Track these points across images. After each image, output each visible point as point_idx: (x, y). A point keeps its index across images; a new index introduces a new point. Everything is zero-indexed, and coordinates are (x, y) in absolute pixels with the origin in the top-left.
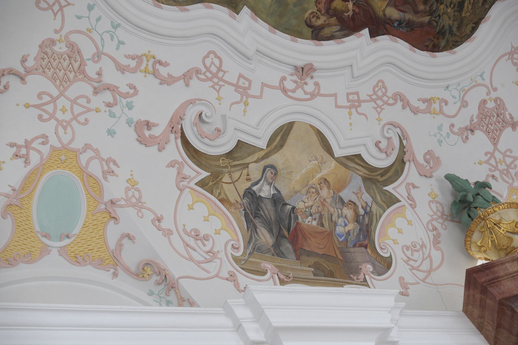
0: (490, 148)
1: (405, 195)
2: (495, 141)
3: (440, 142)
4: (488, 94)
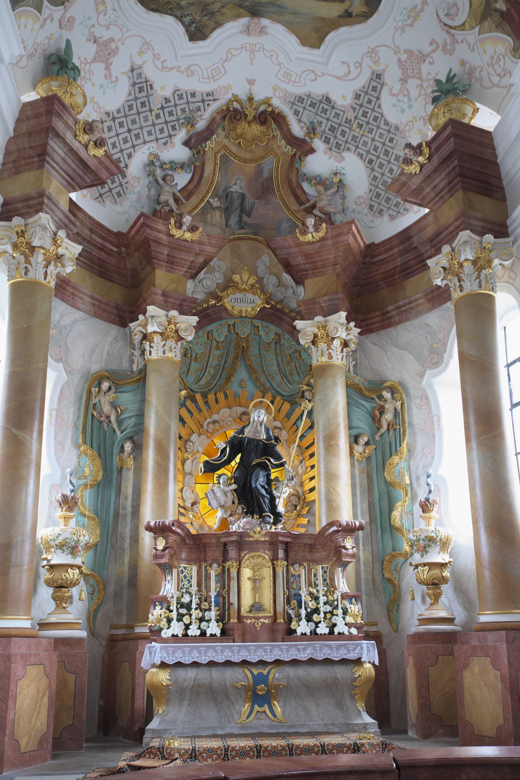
0: (89, 60)
1: (45, 17)
2: (94, 61)
3: (81, 23)
4: (119, 40)
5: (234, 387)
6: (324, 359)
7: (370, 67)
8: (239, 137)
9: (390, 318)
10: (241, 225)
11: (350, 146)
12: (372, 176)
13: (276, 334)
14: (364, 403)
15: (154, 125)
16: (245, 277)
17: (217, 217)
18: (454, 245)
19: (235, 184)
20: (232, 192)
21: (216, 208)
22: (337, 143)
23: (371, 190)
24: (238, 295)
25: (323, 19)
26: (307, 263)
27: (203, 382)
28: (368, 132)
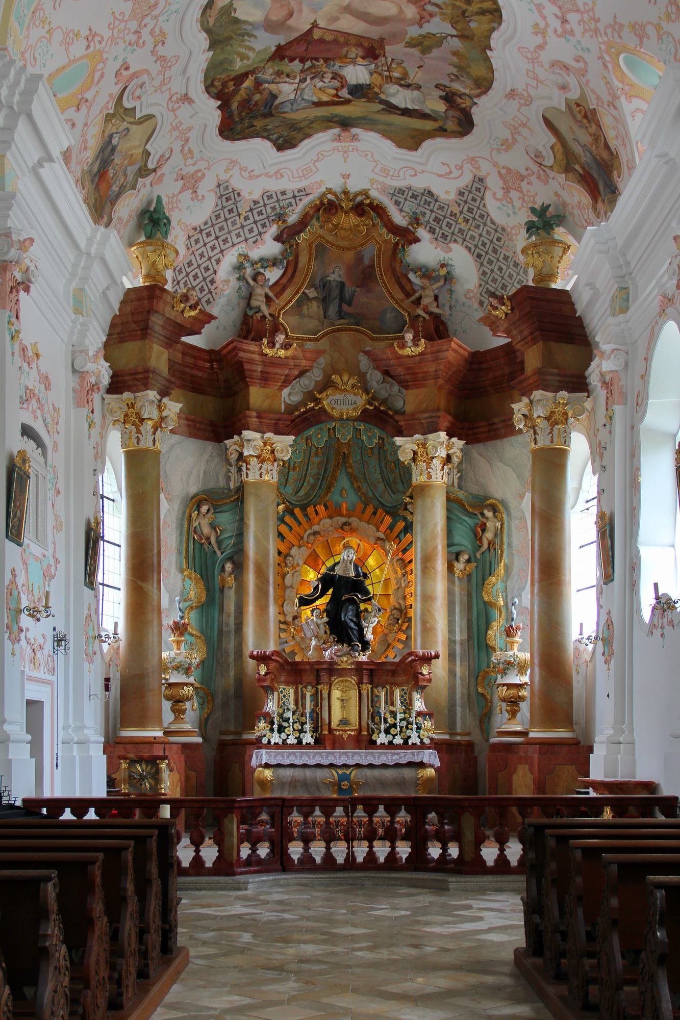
5: (334, 497)
6: (423, 479)
7: (471, 171)
8: (336, 226)
9: (496, 430)
10: (341, 315)
11: (457, 238)
12: (481, 271)
13: (380, 437)
14: (466, 519)
15: (242, 227)
16: (345, 378)
17: (314, 308)
18: (532, 397)
19: (333, 273)
20: (330, 281)
21: (313, 298)
22: (443, 234)
23: (480, 285)
24: (339, 396)
25: (418, 130)
26: (409, 374)
27: (302, 493)
28: (475, 227)
